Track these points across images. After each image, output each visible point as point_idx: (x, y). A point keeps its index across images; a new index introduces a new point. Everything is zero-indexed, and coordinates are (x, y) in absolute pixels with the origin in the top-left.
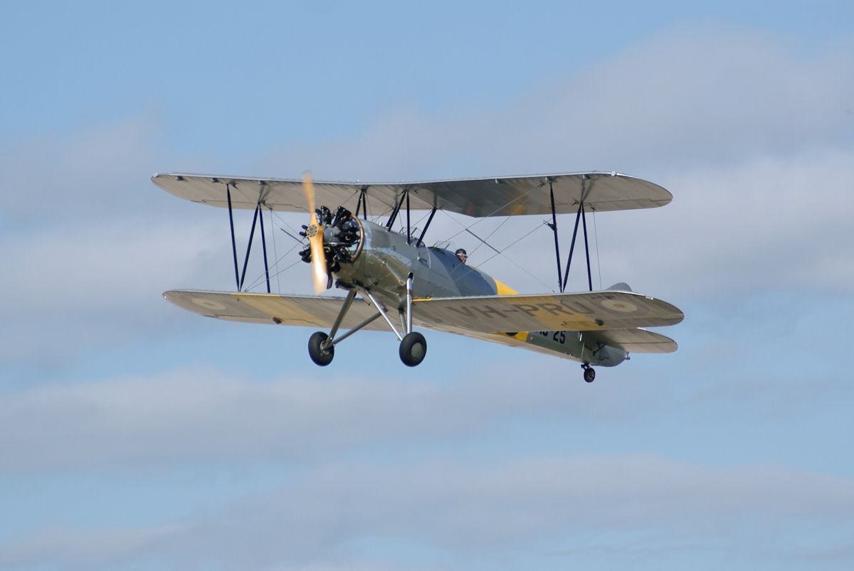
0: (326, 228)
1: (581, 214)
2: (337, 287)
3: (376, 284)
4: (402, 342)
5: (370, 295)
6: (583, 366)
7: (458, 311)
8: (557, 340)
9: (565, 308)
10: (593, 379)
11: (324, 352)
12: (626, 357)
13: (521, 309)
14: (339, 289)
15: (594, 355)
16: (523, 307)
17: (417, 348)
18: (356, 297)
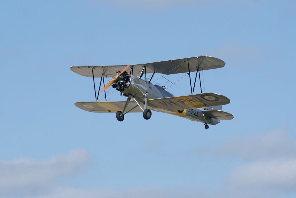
1: (198, 71)
2: (124, 96)
3: (136, 95)
4: (144, 112)
5: (134, 98)
6: (205, 124)
8: (196, 115)
10: (208, 128)
11: (121, 117)
12: (219, 122)
13: (181, 101)
14: (124, 97)
16: (181, 100)
17: (148, 114)
18: (131, 100)
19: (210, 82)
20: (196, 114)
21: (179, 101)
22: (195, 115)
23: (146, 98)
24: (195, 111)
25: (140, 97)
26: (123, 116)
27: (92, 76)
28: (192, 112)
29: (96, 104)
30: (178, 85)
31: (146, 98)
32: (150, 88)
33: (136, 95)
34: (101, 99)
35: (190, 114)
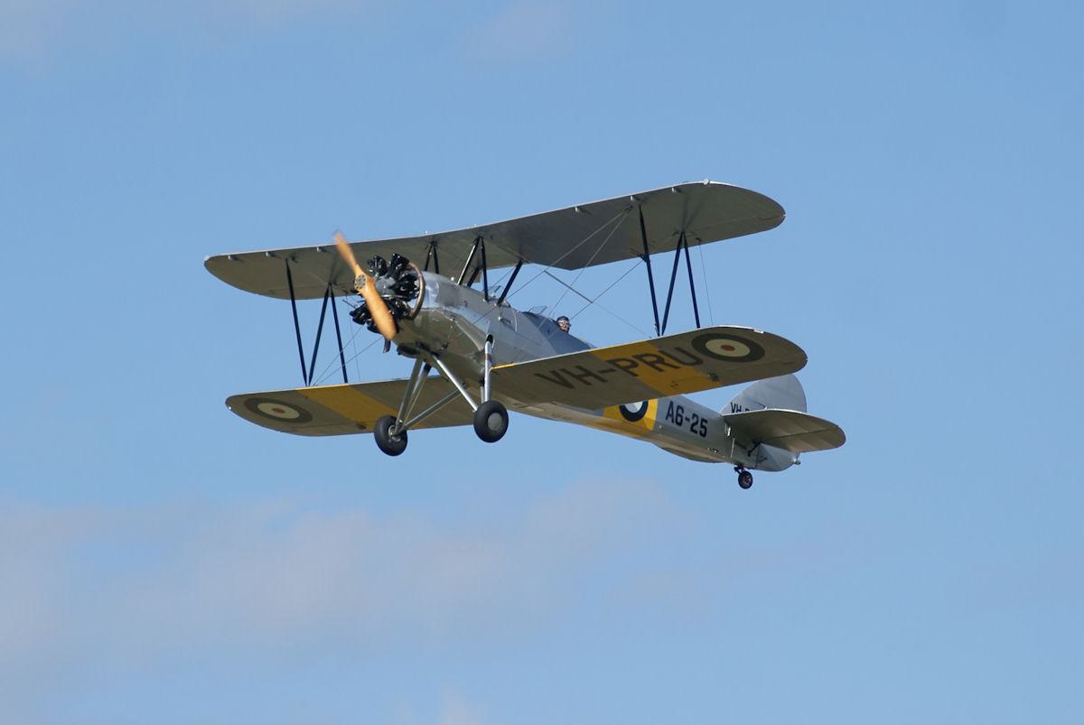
0: (378, 279)
1: (683, 251)
3: (446, 347)
5: (438, 362)
6: (736, 469)
7: (550, 379)
8: (696, 432)
9: (667, 360)
10: (751, 484)
11: (393, 438)
12: (795, 460)
13: (618, 366)
15: (749, 455)
16: (618, 363)
17: (494, 420)
18: (430, 374)
19: (728, 285)
20: (697, 428)
21: (615, 368)
22: (692, 430)
23: (486, 361)
24: (694, 415)
25: (466, 356)
26: (403, 436)
27: (289, 292)
28: (679, 420)
29: (307, 398)
30: (608, 306)
31: (486, 361)
32: (505, 324)
33: (448, 349)
34: (328, 377)
35: (675, 425)
